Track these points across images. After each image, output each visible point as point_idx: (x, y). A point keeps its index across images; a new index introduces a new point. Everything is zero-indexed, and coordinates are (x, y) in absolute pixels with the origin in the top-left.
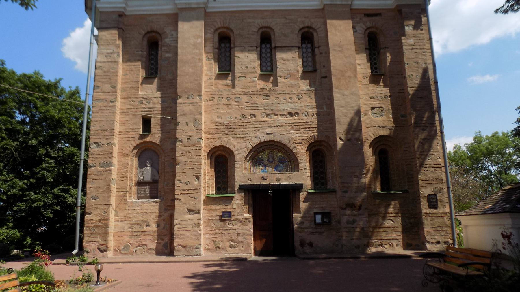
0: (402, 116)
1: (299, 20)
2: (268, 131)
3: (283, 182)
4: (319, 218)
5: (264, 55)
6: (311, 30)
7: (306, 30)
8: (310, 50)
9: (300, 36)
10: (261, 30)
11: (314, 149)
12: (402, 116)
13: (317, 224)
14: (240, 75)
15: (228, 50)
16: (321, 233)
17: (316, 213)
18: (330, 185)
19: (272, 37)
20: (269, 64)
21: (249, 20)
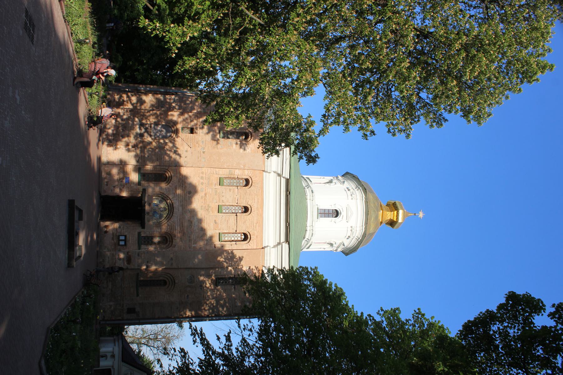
0: (188, 296)
1: (255, 232)
2: (181, 208)
3: (146, 217)
4: (122, 238)
5: (233, 208)
6: (248, 240)
7: (249, 236)
8: (236, 239)
9: (245, 232)
10: (249, 207)
11: (168, 237)
12: (188, 296)
13: (119, 236)
14: (218, 192)
15: (238, 185)
16: (113, 239)
17: (125, 236)
18: (143, 246)
19: (244, 214)
20: (227, 211)
21: (256, 199)
